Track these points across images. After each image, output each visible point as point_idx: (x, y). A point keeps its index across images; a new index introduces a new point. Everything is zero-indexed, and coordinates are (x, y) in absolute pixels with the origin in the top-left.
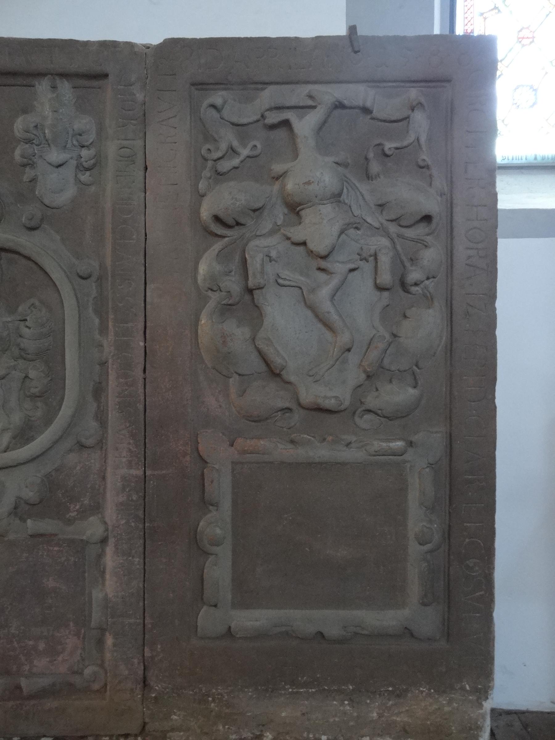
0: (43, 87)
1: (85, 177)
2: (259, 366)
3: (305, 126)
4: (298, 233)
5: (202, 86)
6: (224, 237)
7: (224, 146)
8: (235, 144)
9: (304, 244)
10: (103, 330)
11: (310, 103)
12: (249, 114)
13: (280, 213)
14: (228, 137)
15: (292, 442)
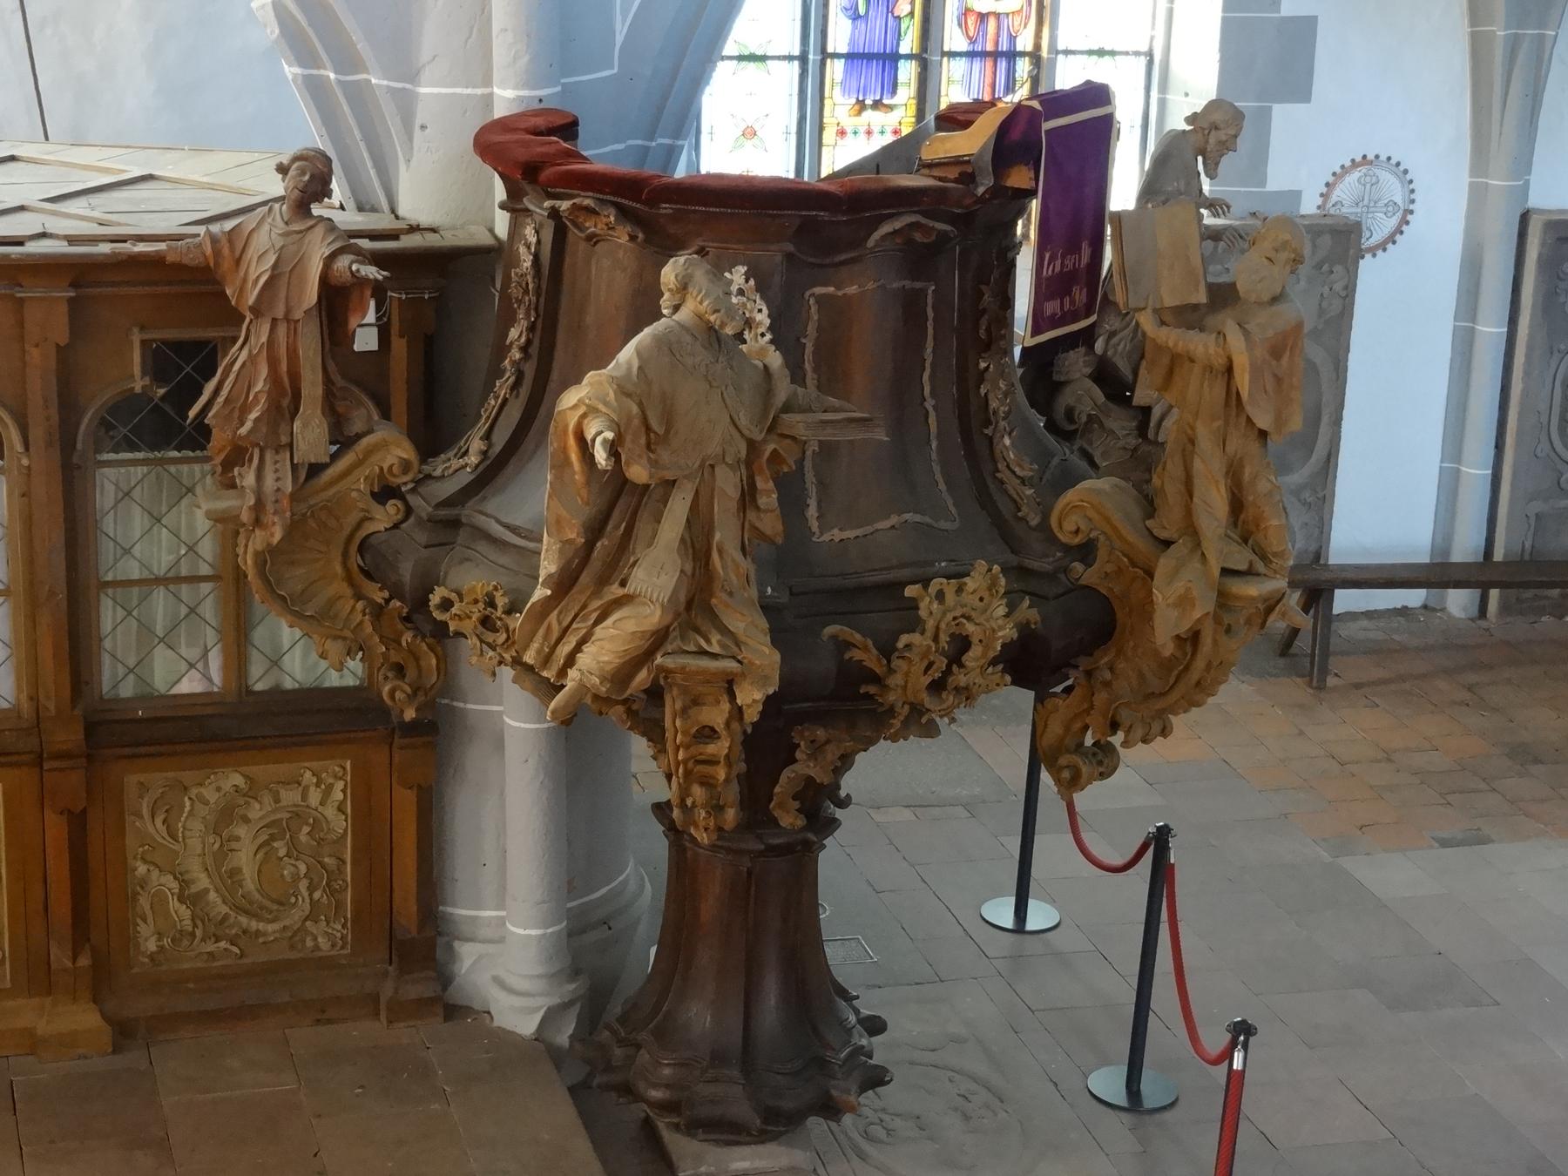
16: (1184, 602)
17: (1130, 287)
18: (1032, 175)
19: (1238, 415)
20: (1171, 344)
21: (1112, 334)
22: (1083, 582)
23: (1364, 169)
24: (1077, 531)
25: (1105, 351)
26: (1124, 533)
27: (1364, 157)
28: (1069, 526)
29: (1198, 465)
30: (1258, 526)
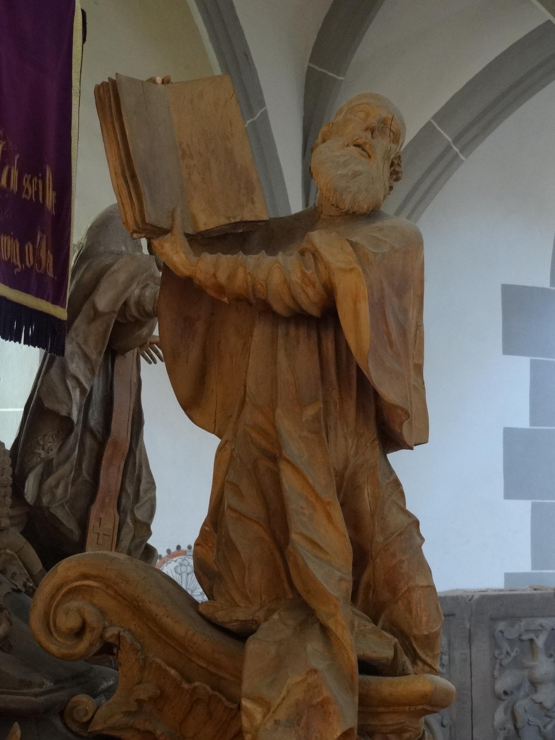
3: (540, 642)
5: (494, 620)
6: (504, 700)
8: (509, 650)
9: (541, 703)
11: (540, 628)
12: (513, 633)
14: (506, 646)
17: (144, 189)
19: (341, 399)
20: (222, 278)
21: (48, 469)
22: (97, 727)
23: (179, 559)
24: (79, 633)
25: (39, 497)
26: (168, 621)
27: (179, 547)
29: (289, 480)
30: (394, 591)
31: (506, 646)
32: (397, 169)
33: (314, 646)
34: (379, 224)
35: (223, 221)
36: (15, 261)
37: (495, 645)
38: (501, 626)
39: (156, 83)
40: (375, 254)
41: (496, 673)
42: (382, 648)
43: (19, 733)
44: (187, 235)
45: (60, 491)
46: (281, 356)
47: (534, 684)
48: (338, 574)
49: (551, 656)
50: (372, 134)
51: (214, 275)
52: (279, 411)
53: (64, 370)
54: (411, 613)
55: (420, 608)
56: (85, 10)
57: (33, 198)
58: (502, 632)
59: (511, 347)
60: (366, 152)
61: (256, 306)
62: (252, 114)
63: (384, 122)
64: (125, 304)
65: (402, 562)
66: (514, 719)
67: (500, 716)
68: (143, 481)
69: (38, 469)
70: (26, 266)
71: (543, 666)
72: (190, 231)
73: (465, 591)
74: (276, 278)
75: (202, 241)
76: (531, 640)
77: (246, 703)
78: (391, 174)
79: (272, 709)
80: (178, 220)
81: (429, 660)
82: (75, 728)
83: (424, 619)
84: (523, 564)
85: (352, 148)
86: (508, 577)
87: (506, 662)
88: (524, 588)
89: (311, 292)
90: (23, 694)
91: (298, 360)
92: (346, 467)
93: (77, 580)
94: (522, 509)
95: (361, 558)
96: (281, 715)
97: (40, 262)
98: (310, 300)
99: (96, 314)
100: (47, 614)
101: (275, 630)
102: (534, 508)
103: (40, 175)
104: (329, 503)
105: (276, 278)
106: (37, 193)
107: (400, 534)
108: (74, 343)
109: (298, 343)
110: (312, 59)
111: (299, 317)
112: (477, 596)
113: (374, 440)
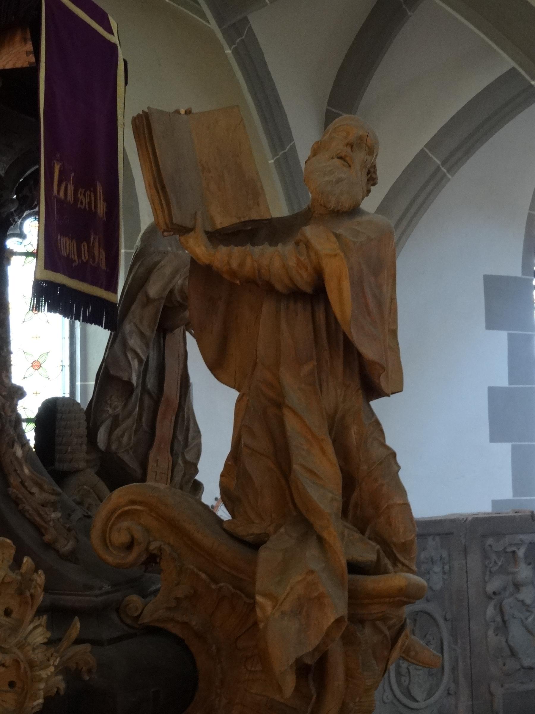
0: (430, 539)
1: (446, 577)
2: (509, 653)
3: (521, 553)
4: (521, 596)
5: (484, 536)
6: (493, 599)
7: (493, 561)
9: (522, 601)
10: (456, 643)
11: (520, 542)
13: (511, 588)
14: (494, 557)
15: (522, 683)
16: (308, 603)
18: (29, 46)
20: (234, 264)
21: (116, 423)
22: (146, 620)
24: (129, 546)
28: (120, 537)
29: (291, 423)
31: (494, 557)
32: (374, 176)
33: (312, 552)
34: (358, 219)
35: (235, 220)
36: (73, 256)
37: (485, 556)
38: (490, 541)
39: (180, 114)
40: (355, 243)
41: (487, 578)
42: (367, 552)
43: (78, 625)
44: (207, 233)
45: (125, 439)
46: (284, 325)
47: (517, 586)
48: (330, 495)
49: (529, 564)
50: (352, 148)
51: (228, 263)
52: (282, 369)
53: (124, 344)
54: (390, 525)
55: (398, 521)
56: (126, 59)
57: (87, 207)
58: (490, 546)
59: (492, 323)
60: (347, 163)
61: (261, 286)
62: (283, 148)
63: (361, 138)
64: (171, 291)
65: (383, 485)
66: (502, 612)
67: (490, 611)
68: (191, 431)
69: (108, 422)
70: (82, 261)
71: (524, 572)
72: (209, 229)
73: (461, 515)
74: (277, 264)
75: (219, 237)
76: (514, 552)
77: (259, 599)
78: (368, 180)
79: (279, 602)
80: (199, 219)
81: (407, 562)
82: (129, 621)
83: (402, 530)
84: (506, 492)
85: (336, 160)
86: (495, 503)
87: (494, 569)
88: (507, 511)
89: (305, 275)
90: (82, 595)
91: (296, 329)
92: (336, 412)
93: (127, 505)
94: (504, 450)
95: (349, 482)
96: (286, 607)
97: (94, 258)
98: (304, 280)
99: (149, 301)
100: (104, 532)
101: (282, 540)
102: (514, 448)
103: (92, 189)
104: (323, 440)
105: (277, 264)
106: (90, 203)
107: (381, 463)
108: (132, 324)
109: (297, 315)
110: (330, 103)
111: (296, 294)
112: (470, 519)
113: (359, 389)
